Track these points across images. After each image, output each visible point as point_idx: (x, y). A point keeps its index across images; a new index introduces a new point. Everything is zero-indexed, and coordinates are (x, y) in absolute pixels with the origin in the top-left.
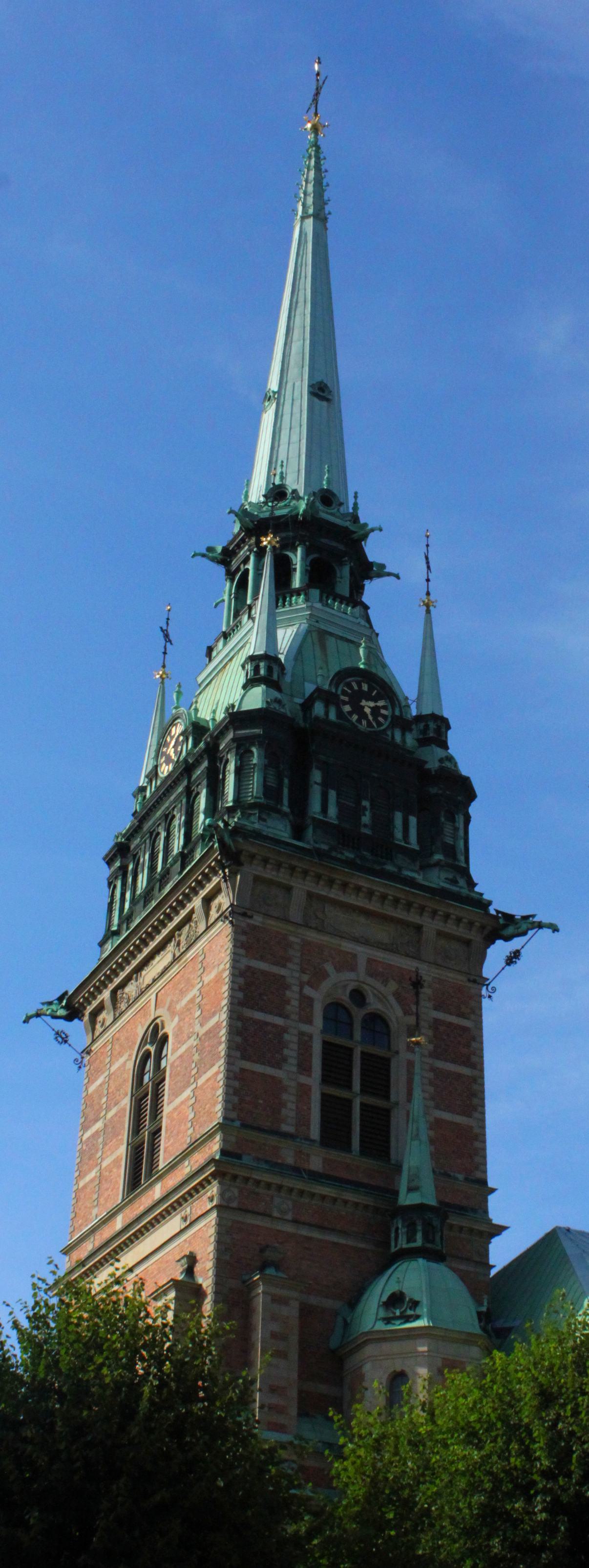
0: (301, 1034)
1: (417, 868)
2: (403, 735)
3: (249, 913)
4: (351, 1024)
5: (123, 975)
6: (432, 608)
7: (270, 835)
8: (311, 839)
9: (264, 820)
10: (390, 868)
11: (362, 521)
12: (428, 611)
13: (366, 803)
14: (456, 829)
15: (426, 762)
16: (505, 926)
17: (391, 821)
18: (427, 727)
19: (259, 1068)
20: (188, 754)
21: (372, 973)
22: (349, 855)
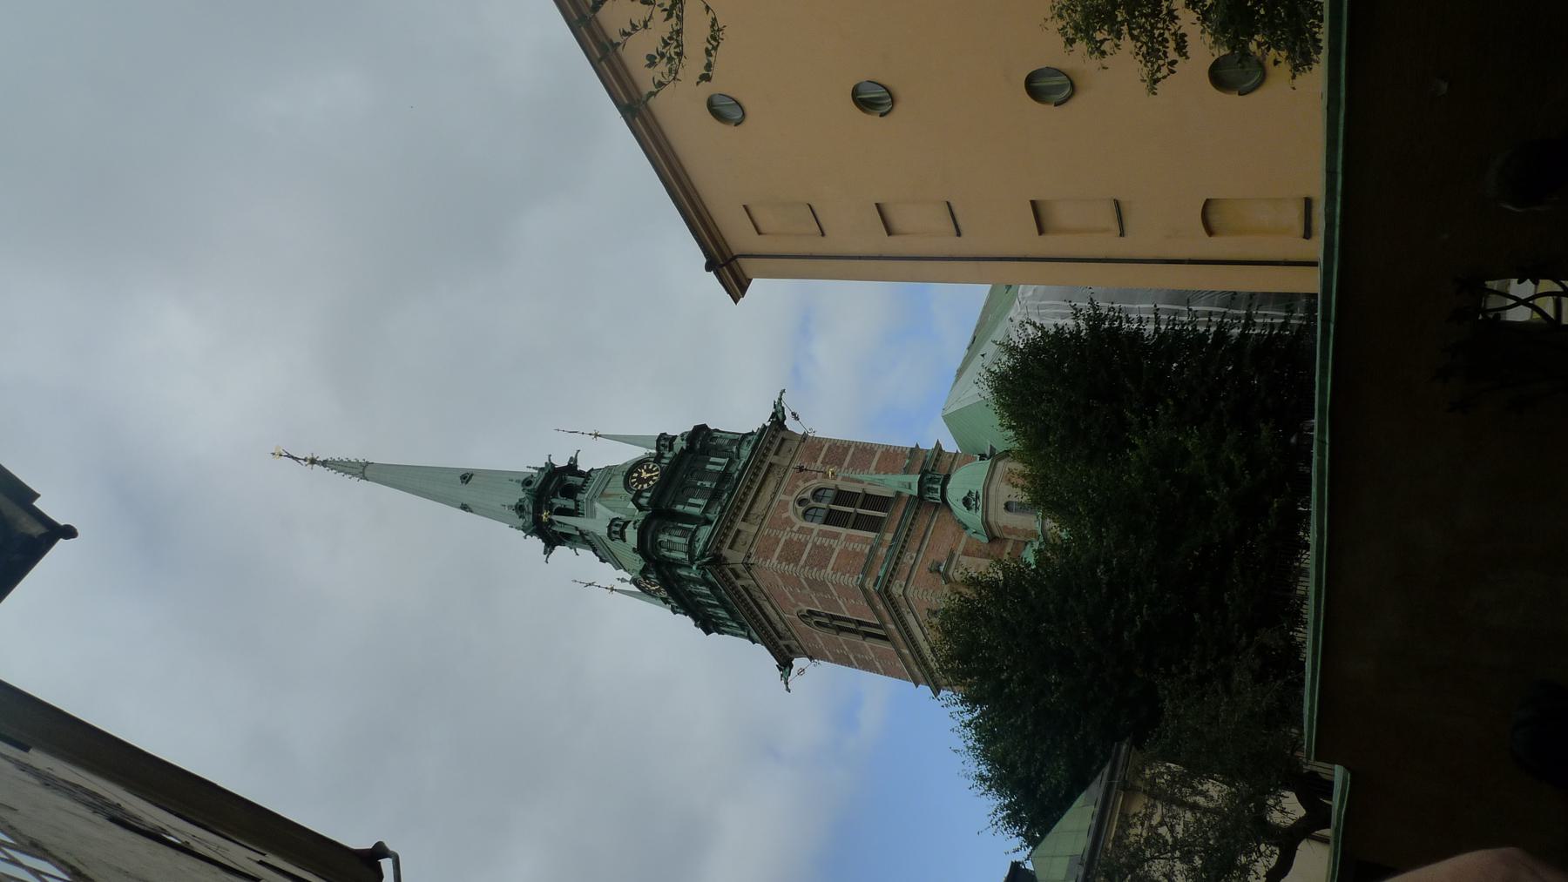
0: (818, 535)
2: (665, 458)
4: (817, 508)
5: (772, 632)
8: (713, 515)
10: (736, 475)
11: (544, 466)
12: (600, 436)
14: (721, 437)
15: (682, 448)
16: (778, 418)
17: (711, 471)
18: (663, 445)
19: (832, 561)
20: (657, 578)
21: (792, 492)
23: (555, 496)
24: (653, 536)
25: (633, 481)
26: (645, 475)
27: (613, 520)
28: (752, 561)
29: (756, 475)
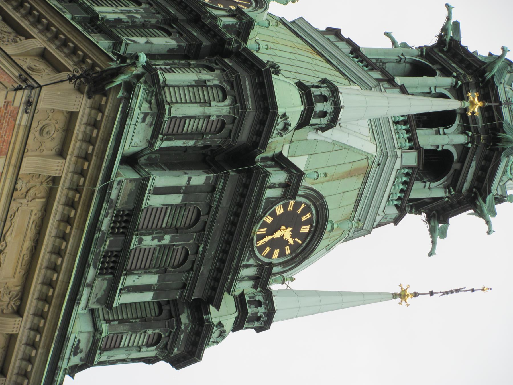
1: (92, 306)
2: (250, 278)
3: (31, 109)
6: (399, 299)
7: (126, 127)
9: (144, 120)
10: (91, 273)
11: (498, 207)
12: (395, 296)
13: (167, 239)
14: (139, 348)
15: (218, 308)
17: (147, 271)
18: (259, 304)
20: (215, 18)
22: (105, 224)
23: (463, 149)
24: (244, 107)
25: (309, 215)
26: (286, 233)
27: (333, 122)
28: (21, 97)
29: (50, 284)
